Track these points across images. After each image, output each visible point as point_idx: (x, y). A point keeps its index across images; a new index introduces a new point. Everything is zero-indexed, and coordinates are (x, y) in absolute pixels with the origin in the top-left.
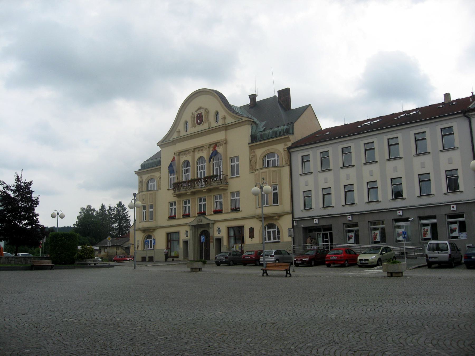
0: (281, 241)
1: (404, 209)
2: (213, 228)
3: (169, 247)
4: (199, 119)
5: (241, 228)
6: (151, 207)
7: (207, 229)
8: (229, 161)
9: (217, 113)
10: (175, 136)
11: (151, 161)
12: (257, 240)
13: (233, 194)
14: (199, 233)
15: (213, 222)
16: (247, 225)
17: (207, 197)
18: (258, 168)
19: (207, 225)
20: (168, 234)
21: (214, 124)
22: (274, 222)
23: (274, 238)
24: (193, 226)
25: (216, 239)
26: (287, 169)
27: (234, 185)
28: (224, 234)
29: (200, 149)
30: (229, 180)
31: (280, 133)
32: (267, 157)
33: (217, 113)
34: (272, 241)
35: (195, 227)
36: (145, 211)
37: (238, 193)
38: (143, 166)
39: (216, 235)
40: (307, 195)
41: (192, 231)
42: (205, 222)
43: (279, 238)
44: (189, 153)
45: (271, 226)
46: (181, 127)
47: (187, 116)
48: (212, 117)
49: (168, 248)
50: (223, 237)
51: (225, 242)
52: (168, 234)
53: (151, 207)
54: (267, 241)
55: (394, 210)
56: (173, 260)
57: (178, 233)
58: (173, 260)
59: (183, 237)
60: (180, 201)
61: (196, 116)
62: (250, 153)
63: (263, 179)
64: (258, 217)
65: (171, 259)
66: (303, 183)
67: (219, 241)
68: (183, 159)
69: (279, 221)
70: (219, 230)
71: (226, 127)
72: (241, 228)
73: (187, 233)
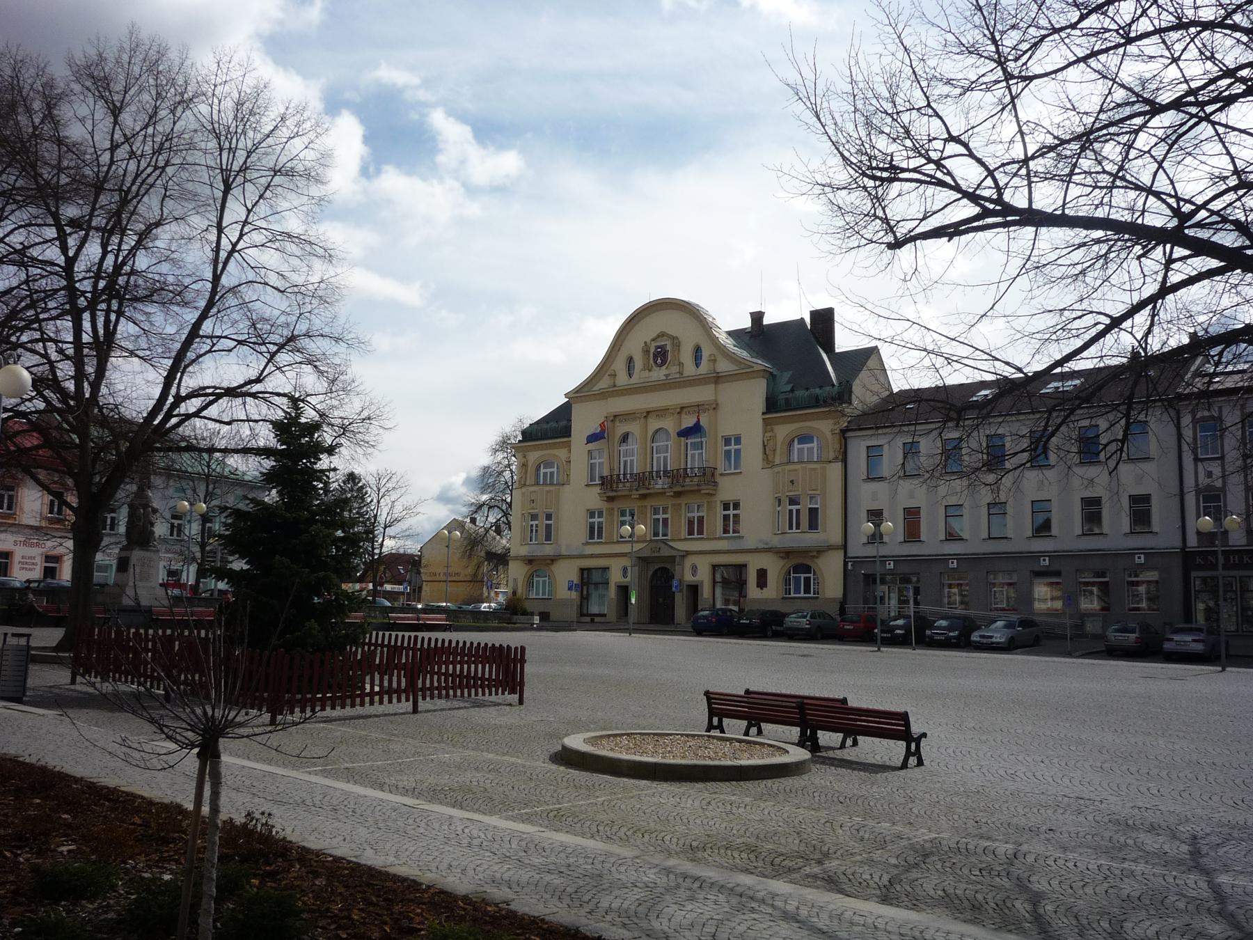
1: (1054, 556)
2: (682, 564)
4: (660, 356)
5: (742, 567)
6: (549, 517)
7: (668, 566)
8: (721, 442)
9: (698, 350)
10: (604, 383)
11: (545, 426)
12: (772, 591)
13: (726, 506)
14: (650, 573)
16: (754, 564)
18: (777, 461)
19: (672, 559)
20: (582, 570)
21: (690, 369)
23: (807, 591)
25: (688, 586)
26: (837, 467)
27: (728, 489)
30: (718, 479)
33: (698, 350)
35: (643, 561)
36: (534, 523)
39: (688, 578)
42: (666, 552)
44: (635, 419)
45: (799, 568)
46: (620, 365)
47: (634, 347)
48: (687, 356)
51: (706, 592)
53: (549, 517)
54: (792, 595)
55: (1036, 556)
56: (592, 621)
57: (605, 569)
58: (592, 621)
59: (616, 577)
61: (652, 350)
62: (765, 432)
63: (792, 482)
65: (588, 619)
66: (867, 495)
67: (694, 589)
68: (621, 429)
70: (694, 569)
72: (742, 567)
73: (625, 570)
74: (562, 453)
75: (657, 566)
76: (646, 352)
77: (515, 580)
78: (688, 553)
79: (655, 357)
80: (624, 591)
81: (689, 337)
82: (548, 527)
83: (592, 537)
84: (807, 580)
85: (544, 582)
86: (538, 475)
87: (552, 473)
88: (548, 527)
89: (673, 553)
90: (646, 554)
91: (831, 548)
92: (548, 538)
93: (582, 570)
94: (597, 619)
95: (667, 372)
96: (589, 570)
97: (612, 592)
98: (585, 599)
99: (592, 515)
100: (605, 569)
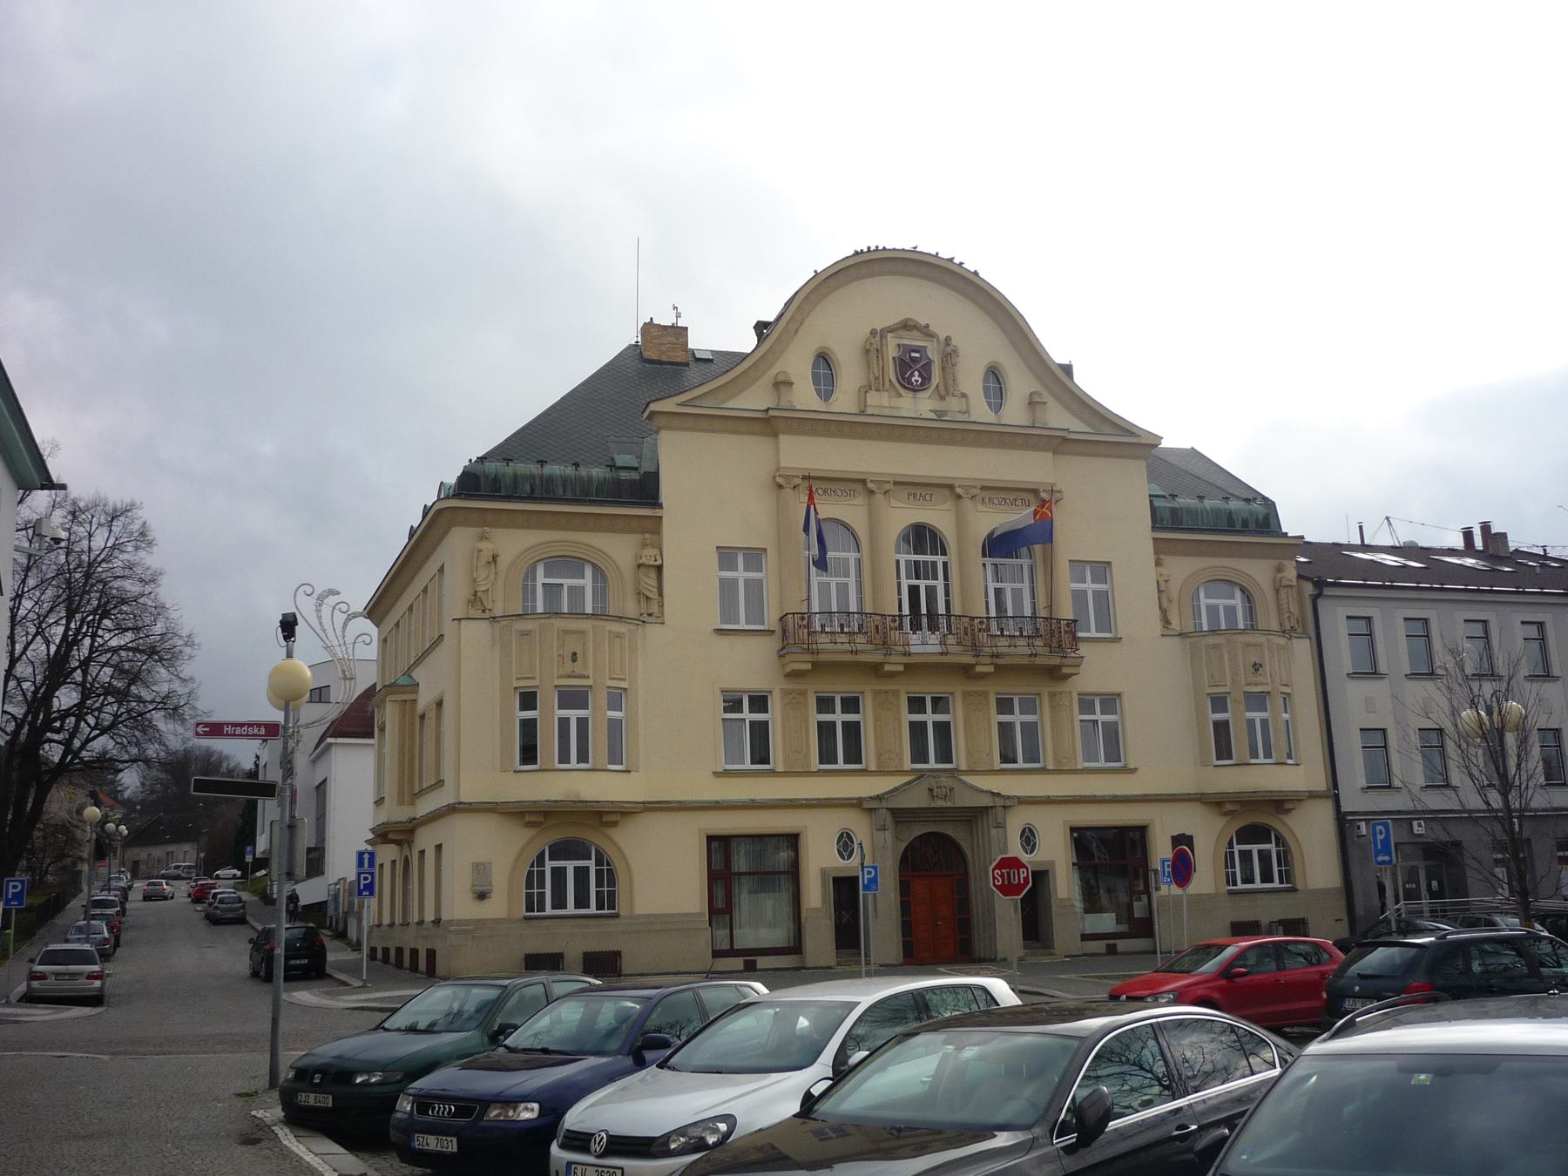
0: (1299, 886)
2: (1001, 826)
3: (720, 904)
7: (948, 830)
9: (994, 374)
11: (492, 467)
13: (1086, 704)
14: (904, 845)
15: (1008, 803)
16: (1163, 829)
17: (966, 695)
19: (974, 816)
20: (710, 839)
21: (981, 411)
22: (1274, 822)
24: (893, 811)
26: (1302, 649)
28: (1054, 851)
31: (1245, 523)
32: (1202, 594)
33: (994, 374)
34: (1258, 885)
37: (1111, 701)
38: (472, 483)
40: (1376, 741)
41: (889, 835)
43: (1286, 876)
44: (851, 494)
46: (797, 364)
48: (971, 380)
49: (713, 911)
50: (1052, 863)
52: (719, 845)
53: (615, 700)
54: (1240, 886)
57: (792, 840)
59: (820, 858)
60: (803, 693)
61: (892, 352)
63: (1257, 667)
64: (1216, 803)
65: (738, 963)
66: (1360, 704)
69: (1287, 819)
70: (1029, 838)
71: (1061, 444)
73: (845, 843)
74: (619, 549)
75: (918, 830)
76: (871, 350)
77: (481, 869)
78: (1023, 801)
80: (845, 890)
81: (977, 346)
82: (615, 727)
84: (1265, 857)
85: (582, 874)
86: (528, 592)
87: (577, 593)
88: (615, 727)
90: (917, 799)
91: (1313, 795)
92: (615, 755)
93: (710, 839)
94: (763, 962)
95: (938, 405)
97: (815, 895)
98: (721, 909)
100: (792, 840)
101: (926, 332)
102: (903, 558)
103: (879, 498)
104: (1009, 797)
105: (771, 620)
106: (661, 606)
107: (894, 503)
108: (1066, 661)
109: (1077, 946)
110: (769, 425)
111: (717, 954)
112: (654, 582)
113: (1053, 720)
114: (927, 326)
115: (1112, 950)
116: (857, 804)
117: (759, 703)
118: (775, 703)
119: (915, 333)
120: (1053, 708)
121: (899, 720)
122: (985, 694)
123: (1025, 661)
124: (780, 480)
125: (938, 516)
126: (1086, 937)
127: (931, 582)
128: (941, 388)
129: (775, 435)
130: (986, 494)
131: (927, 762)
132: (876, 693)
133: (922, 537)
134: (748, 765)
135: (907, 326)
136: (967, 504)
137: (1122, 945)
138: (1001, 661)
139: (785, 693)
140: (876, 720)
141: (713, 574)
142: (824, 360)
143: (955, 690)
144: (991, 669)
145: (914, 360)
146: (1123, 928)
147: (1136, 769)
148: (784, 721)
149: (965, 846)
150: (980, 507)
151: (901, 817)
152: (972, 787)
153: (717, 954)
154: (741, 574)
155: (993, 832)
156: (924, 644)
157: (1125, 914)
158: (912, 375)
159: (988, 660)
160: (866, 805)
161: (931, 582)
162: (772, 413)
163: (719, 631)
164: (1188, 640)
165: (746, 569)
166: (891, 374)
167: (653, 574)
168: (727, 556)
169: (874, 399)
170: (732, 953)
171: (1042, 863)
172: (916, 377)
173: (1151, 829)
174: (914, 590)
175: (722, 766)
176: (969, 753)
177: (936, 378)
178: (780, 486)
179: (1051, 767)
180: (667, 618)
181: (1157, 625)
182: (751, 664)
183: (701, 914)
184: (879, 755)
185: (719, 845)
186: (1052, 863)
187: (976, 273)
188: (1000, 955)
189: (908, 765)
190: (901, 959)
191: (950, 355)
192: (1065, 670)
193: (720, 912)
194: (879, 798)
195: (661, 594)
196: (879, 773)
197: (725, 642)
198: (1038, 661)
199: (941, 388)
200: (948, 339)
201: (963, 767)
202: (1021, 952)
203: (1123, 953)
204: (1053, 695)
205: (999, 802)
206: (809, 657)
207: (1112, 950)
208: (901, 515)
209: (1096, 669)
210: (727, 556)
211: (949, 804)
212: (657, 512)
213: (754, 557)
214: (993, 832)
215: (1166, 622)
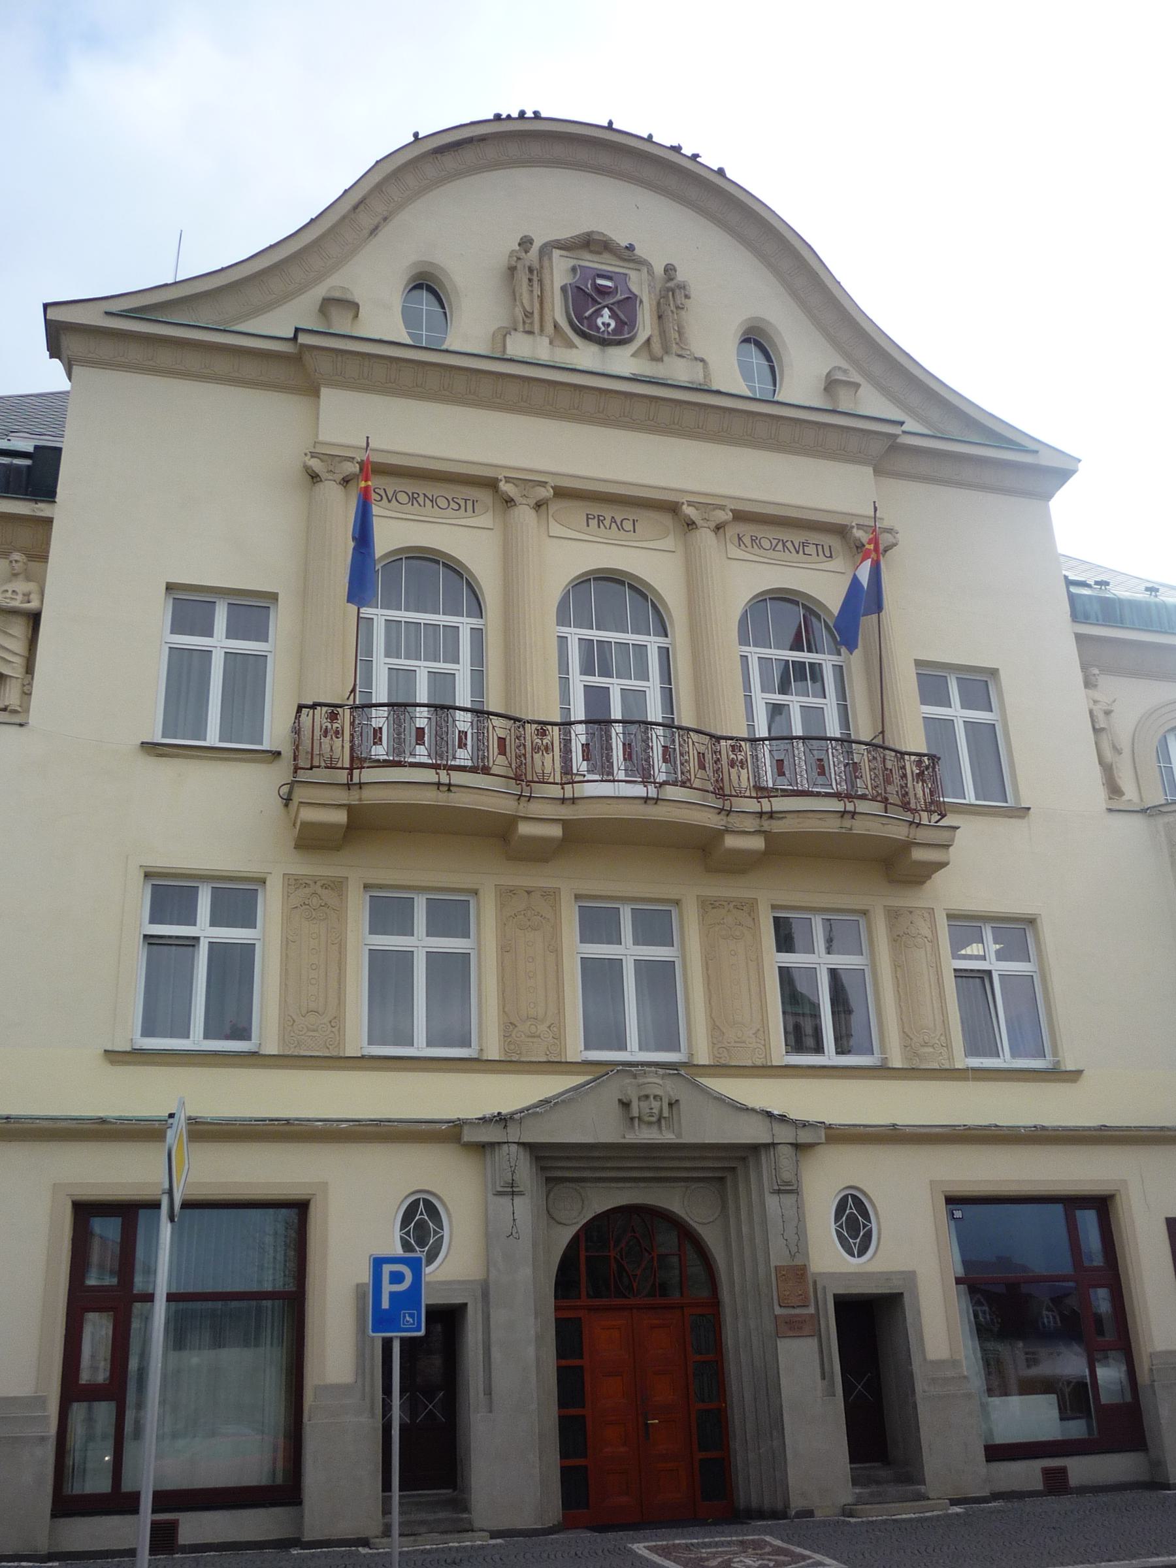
2: (790, 1189)
3: (95, 1365)
7: (673, 1201)
9: (756, 339)
14: (565, 1236)
15: (804, 1137)
19: (729, 1167)
20: (85, 1212)
24: (531, 1148)
29: (608, 512)
37: (1017, 932)
41: (524, 1208)
49: (73, 1390)
51: (940, 1329)
60: (337, 886)
61: (560, 271)
70: (854, 1220)
71: (888, 454)
75: (602, 1200)
76: (523, 269)
79: (586, 298)
83: (162, 1012)
89: (752, 1132)
90: (596, 1125)
93: (85, 1212)
96: (130, 1213)
97: (337, 1348)
99: (170, 894)
101: (627, 254)
102: (575, 634)
103: (524, 515)
104: (805, 1125)
105: (275, 730)
106: (27, 694)
107: (556, 529)
108: (921, 835)
109: (979, 1476)
110: (300, 367)
111: (66, 1505)
112: (18, 645)
113: (897, 966)
114: (630, 248)
115: (1056, 1483)
116: (450, 1134)
117: (237, 900)
118: (271, 905)
119: (607, 257)
120: (899, 941)
121: (557, 952)
122: (749, 906)
123: (832, 826)
124: (315, 464)
125: (651, 560)
126: (996, 1453)
127: (634, 684)
128: (656, 346)
129: (313, 392)
130: (747, 530)
131: (622, 1047)
132: (506, 894)
133: (609, 594)
134: (196, 1040)
135: (590, 243)
136: (705, 538)
137: (1080, 1469)
138: (777, 826)
139: (294, 883)
140: (505, 949)
141: (155, 635)
142: (426, 284)
143: (688, 891)
144: (758, 843)
145: (602, 291)
146: (1077, 1429)
147: (1079, 1073)
148: (287, 943)
149: (711, 1237)
150: (735, 552)
151: (556, 1165)
152: (720, 1099)
153: (66, 1505)
154: (219, 643)
155: (772, 1201)
156: (612, 791)
157: (1076, 1398)
158: (598, 313)
159: (750, 824)
160: (468, 1136)
161: (634, 684)
162: (303, 339)
163: (150, 748)
164: (1161, 821)
165: (231, 634)
166: (558, 311)
167: (19, 629)
168: (190, 606)
169: (519, 346)
170: (121, 1502)
171: (887, 1276)
172: (606, 316)
173: (1118, 1197)
174: (597, 697)
175: (131, 1035)
176: (715, 1029)
177: (646, 326)
178: (314, 477)
179: (897, 1062)
180: (34, 717)
181: (1100, 793)
182: (221, 818)
183: (39, 1401)
184: (508, 1027)
185: (104, 1229)
186: (910, 1277)
187: (721, 172)
188: (797, 1503)
189: (575, 1049)
190: (554, 1513)
191: (672, 292)
192: (918, 854)
193: (93, 1394)
194: (502, 1120)
195: (29, 669)
196: (509, 1065)
197: (167, 769)
198: (860, 827)
199: (656, 346)
200: (669, 270)
201: (703, 1058)
202: (846, 1494)
203: (1082, 1490)
204: (893, 915)
205: (784, 1134)
206: (342, 796)
207: (1056, 1483)
208: (568, 552)
209: (979, 866)
210: (190, 606)
211: (668, 1137)
212: (42, 509)
213: (251, 611)
214: (772, 1201)
215: (1114, 790)
